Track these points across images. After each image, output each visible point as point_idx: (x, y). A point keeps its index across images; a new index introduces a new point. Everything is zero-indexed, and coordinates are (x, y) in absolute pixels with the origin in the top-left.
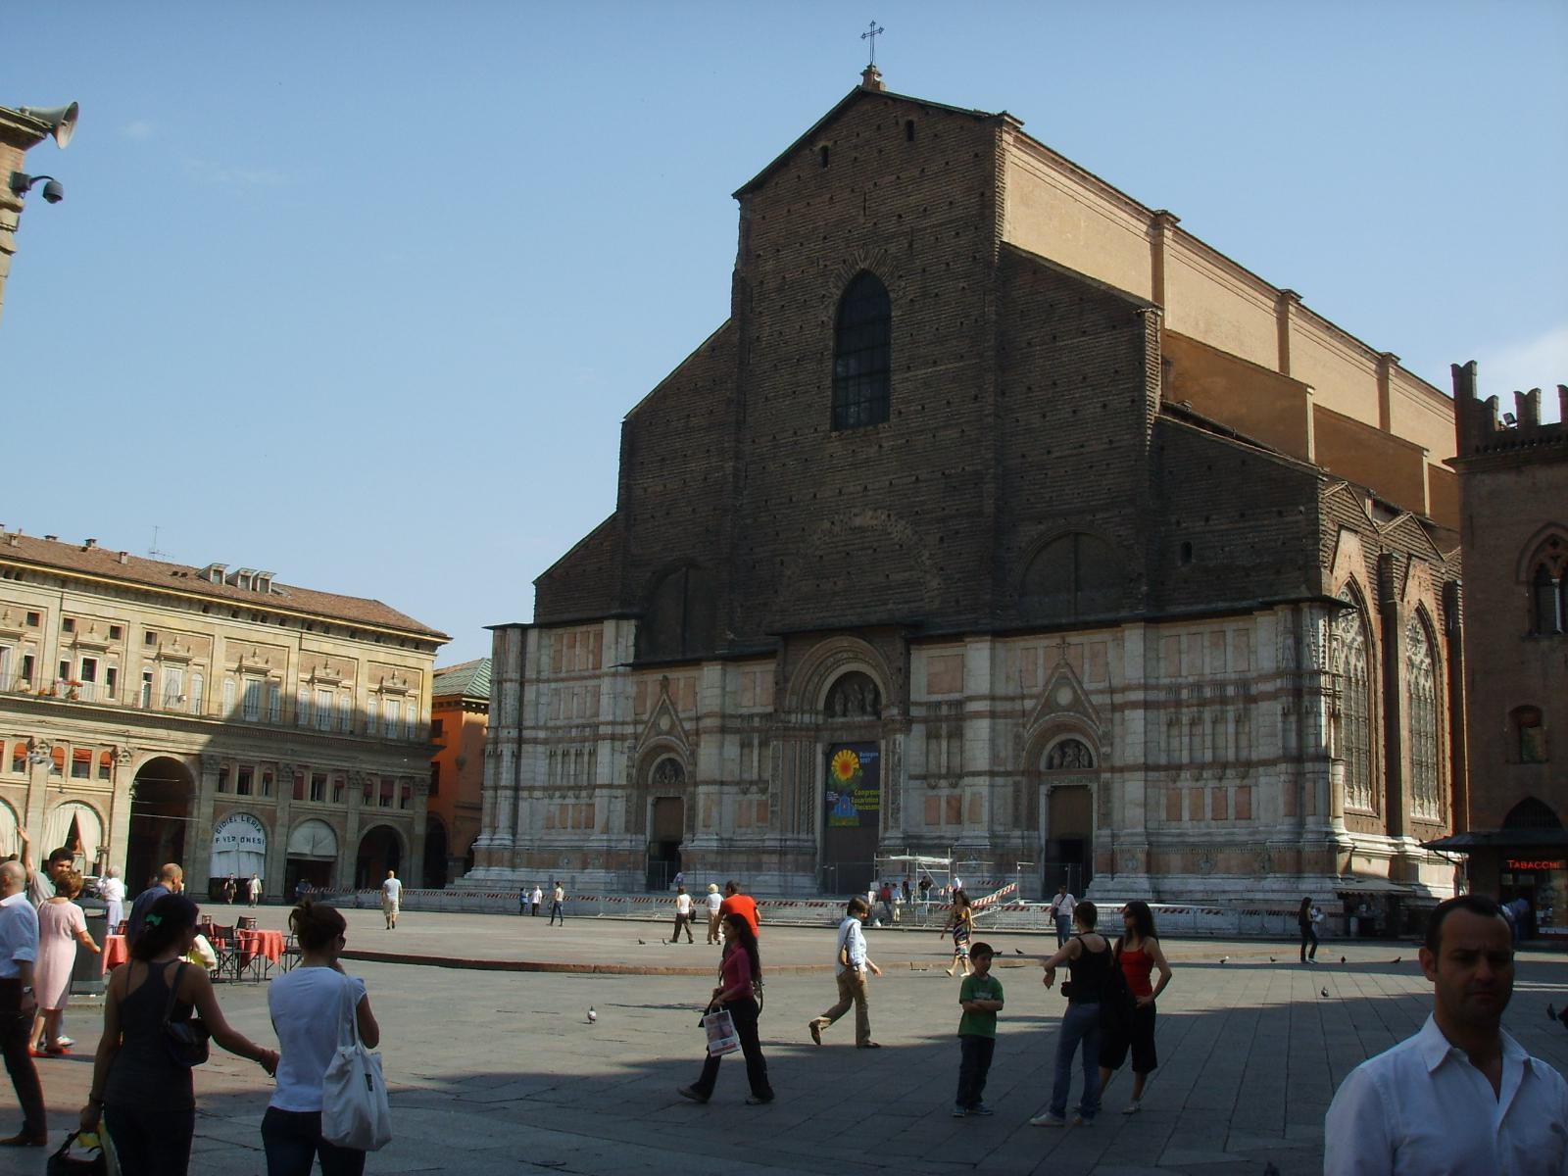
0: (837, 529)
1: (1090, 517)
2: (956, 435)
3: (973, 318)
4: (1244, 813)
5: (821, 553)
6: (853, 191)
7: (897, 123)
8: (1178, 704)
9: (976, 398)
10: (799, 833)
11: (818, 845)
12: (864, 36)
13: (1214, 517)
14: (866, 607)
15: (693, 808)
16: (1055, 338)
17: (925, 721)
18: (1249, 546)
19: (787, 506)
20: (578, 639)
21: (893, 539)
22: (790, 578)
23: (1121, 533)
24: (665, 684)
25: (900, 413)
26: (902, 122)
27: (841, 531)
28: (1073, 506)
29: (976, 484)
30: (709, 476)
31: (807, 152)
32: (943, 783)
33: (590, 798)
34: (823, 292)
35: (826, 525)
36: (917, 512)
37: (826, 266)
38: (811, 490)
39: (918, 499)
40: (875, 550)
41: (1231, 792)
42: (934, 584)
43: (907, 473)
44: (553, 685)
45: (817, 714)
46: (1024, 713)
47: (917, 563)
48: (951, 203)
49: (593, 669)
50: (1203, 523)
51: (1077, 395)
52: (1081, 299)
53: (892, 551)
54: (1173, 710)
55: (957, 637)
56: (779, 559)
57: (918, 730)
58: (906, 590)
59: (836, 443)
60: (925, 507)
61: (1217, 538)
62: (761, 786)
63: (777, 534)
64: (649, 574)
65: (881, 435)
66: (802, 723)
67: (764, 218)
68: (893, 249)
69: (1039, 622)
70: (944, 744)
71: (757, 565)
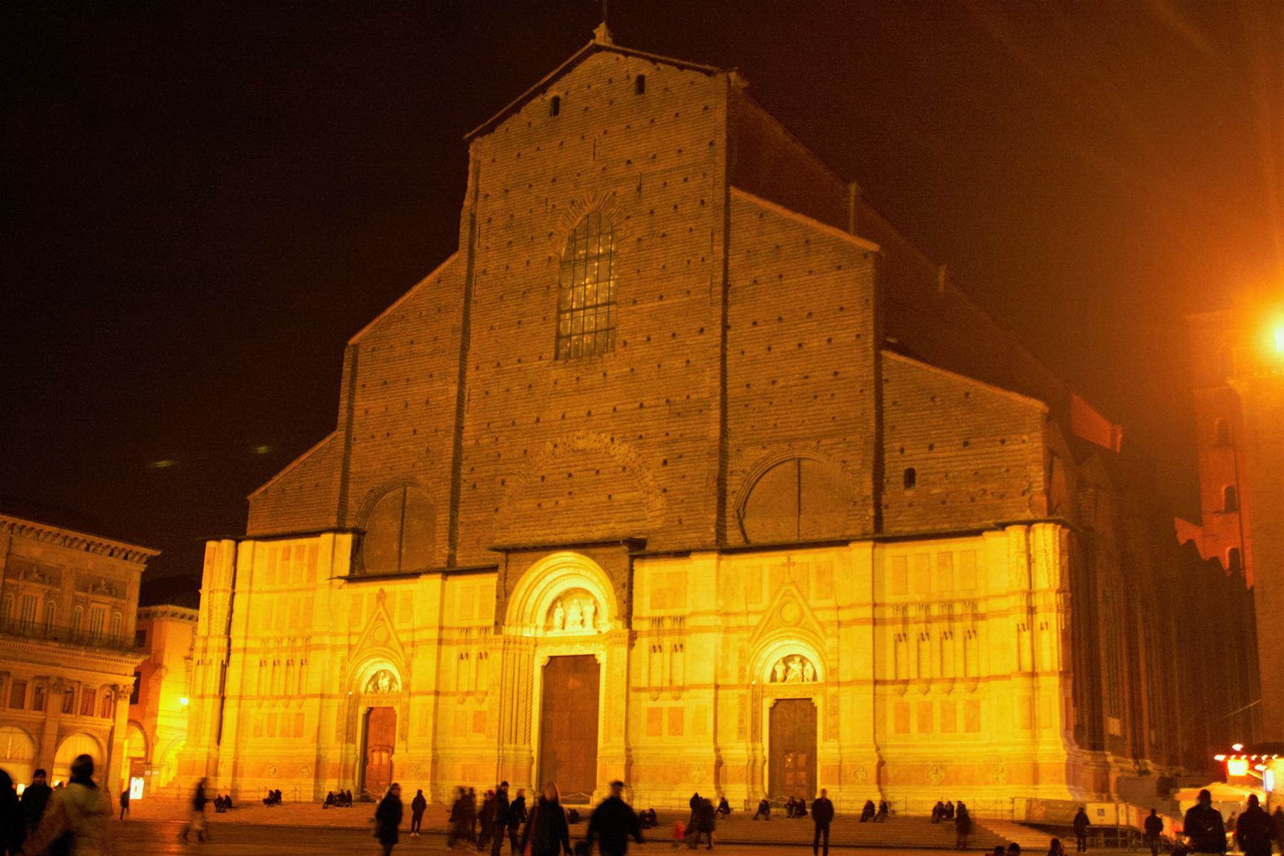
1: (814, 444)
2: (680, 365)
3: (700, 259)
4: (973, 725)
5: (544, 473)
6: (583, 137)
7: (628, 77)
8: (905, 621)
9: (702, 330)
10: (516, 743)
11: (535, 754)
13: (937, 445)
14: (588, 525)
15: (406, 719)
16: (781, 276)
18: (973, 473)
19: (510, 428)
20: (293, 552)
22: (511, 497)
24: (381, 596)
25: (625, 343)
26: (634, 77)
29: (701, 411)
31: (537, 101)
32: (666, 695)
33: (301, 707)
34: (553, 230)
36: (641, 437)
37: (554, 206)
38: (534, 414)
39: (641, 424)
41: (960, 707)
42: (659, 502)
43: (630, 400)
44: (266, 597)
46: (748, 628)
48: (680, 151)
49: (308, 581)
50: (926, 450)
51: (802, 329)
52: (807, 242)
53: (615, 473)
54: (900, 626)
55: (683, 554)
59: (559, 371)
60: (649, 432)
61: (941, 465)
62: (479, 697)
63: (499, 455)
64: (367, 490)
66: (522, 636)
67: (494, 160)
68: (621, 190)
69: (762, 541)
70: (667, 656)
71: (478, 484)
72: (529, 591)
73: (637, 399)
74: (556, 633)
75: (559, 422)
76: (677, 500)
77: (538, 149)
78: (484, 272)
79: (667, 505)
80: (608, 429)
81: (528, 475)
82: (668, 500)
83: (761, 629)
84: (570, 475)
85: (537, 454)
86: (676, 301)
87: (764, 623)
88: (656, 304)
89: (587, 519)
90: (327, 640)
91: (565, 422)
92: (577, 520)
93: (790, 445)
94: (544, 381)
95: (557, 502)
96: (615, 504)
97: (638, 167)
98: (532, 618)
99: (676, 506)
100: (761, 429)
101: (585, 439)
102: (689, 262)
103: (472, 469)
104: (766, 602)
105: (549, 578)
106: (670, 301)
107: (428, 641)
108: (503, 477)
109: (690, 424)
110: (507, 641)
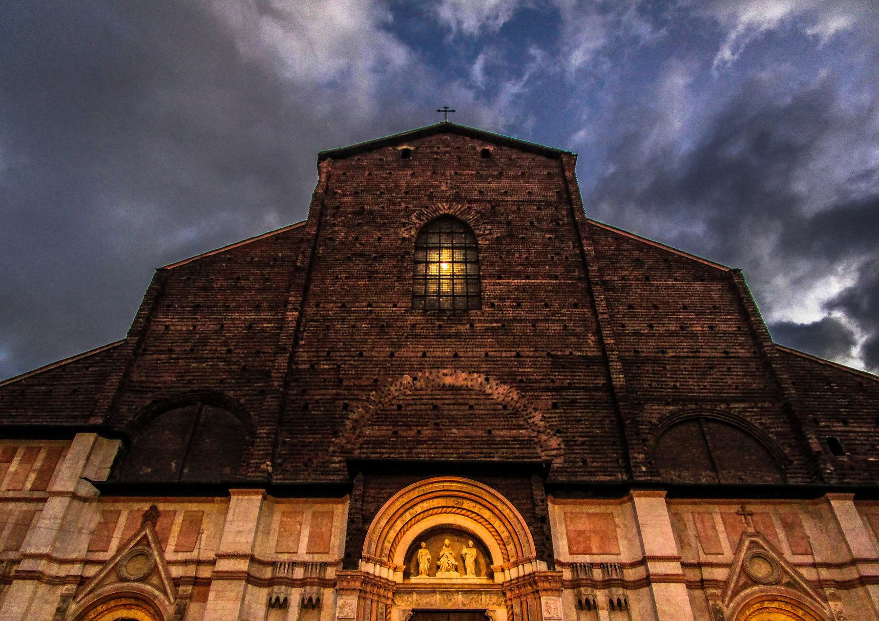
0: (418, 384)
1: (723, 406)
5: (401, 403)
7: (475, 148)
12: (439, 111)
17: (575, 584)
21: (492, 399)
22: (356, 421)
23: (763, 421)
24: (151, 517)
25: (493, 305)
27: (427, 387)
28: (701, 395)
30: (255, 325)
35: (407, 379)
36: (521, 381)
38: (387, 349)
40: (471, 407)
42: (554, 442)
45: (395, 569)
46: (715, 583)
47: (528, 424)
56: (341, 402)
57: (568, 594)
58: (517, 446)
59: (419, 318)
60: (532, 377)
63: (341, 381)
64: (148, 402)
65: (474, 318)
70: (603, 614)
71: (310, 406)
72: (391, 523)
73: (513, 349)
74: (422, 579)
75: (419, 359)
76: (576, 441)
77: (390, 173)
78: (331, 239)
79: (565, 445)
80: (482, 370)
81: (380, 402)
82: (563, 441)
83: (732, 585)
84: (435, 407)
85: (391, 385)
86: (543, 281)
87: (735, 578)
88: (523, 281)
89: (461, 451)
90: (42, 566)
91: (426, 359)
92: (448, 451)
93: (696, 404)
94: (399, 324)
95: (419, 432)
96: (499, 439)
97: (490, 196)
98: (390, 557)
99: (576, 447)
100: (661, 388)
101: (454, 376)
102: (552, 258)
103: (304, 391)
104: (728, 555)
105: (418, 509)
106: (538, 281)
107: (230, 576)
108: (346, 401)
109: (579, 376)
110: (369, 580)
